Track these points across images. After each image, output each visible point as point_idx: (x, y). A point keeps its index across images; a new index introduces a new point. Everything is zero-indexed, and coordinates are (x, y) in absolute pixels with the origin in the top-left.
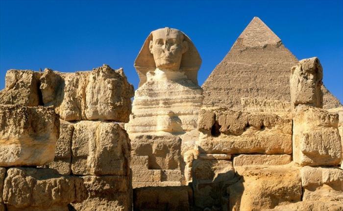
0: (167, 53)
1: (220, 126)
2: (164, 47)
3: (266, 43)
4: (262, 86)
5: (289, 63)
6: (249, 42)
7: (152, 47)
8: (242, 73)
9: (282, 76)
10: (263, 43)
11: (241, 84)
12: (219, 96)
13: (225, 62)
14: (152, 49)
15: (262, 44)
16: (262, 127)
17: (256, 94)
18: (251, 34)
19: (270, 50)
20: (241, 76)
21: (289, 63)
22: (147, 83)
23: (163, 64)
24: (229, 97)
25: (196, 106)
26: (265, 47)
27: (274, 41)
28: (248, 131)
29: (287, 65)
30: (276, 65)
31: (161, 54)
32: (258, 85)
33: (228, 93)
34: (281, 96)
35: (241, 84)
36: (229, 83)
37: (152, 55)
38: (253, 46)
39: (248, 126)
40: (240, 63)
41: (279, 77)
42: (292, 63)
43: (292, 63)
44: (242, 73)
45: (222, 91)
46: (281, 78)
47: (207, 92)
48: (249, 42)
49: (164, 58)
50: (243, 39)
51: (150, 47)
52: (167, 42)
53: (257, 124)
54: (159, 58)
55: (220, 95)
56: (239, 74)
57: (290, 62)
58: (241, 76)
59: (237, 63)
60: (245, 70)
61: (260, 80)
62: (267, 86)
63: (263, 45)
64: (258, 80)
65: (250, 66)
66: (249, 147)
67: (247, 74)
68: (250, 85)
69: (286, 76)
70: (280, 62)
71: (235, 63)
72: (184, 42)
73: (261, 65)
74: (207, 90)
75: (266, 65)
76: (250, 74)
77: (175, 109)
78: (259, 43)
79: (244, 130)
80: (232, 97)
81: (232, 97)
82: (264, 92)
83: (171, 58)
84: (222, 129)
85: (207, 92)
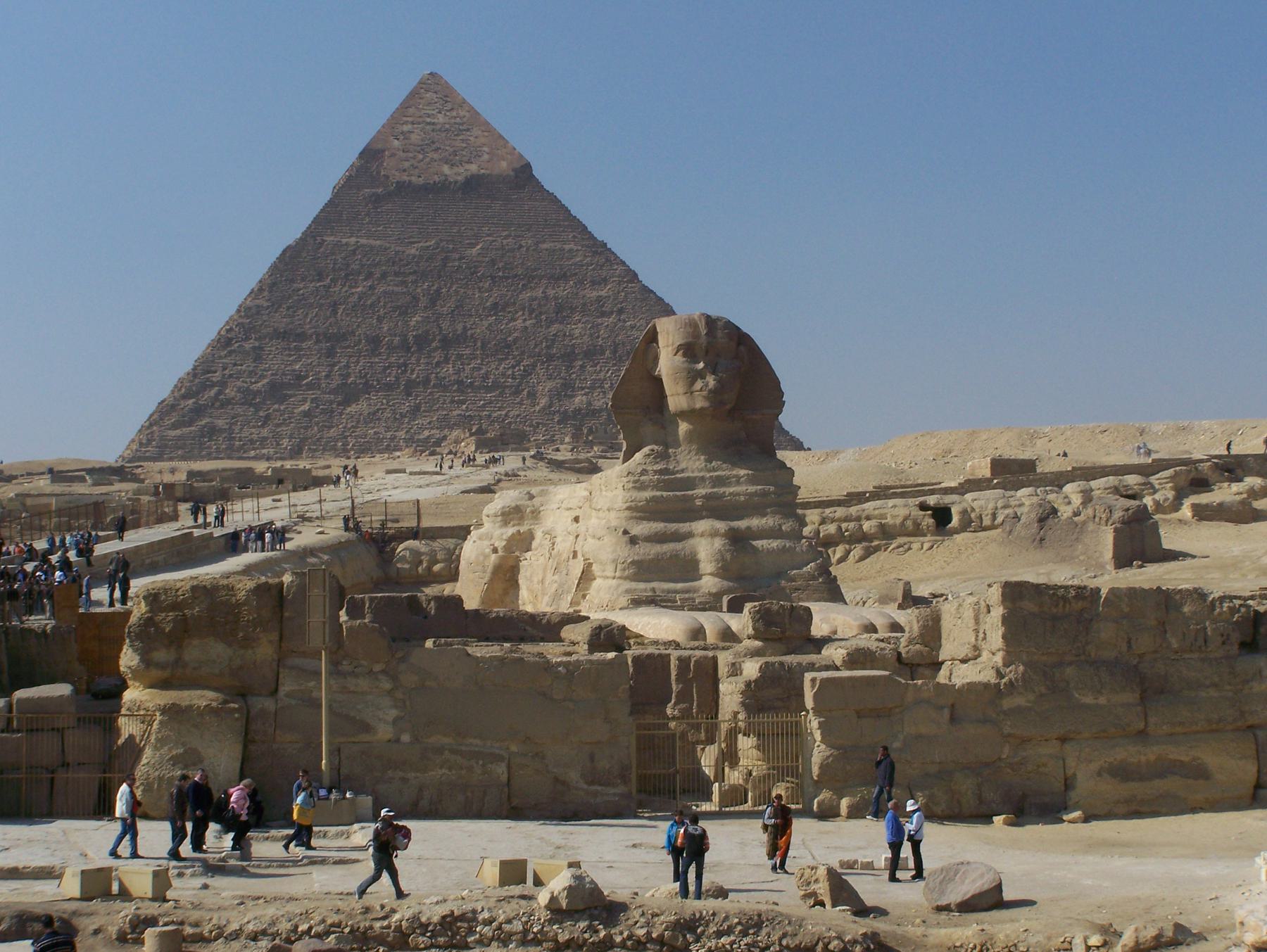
0: (711, 381)
2: (701, 365)
3: (473, 168)
4: (460, 327)
5: (559, 246)
6: (406, 164)
8: (384, 275)
11: (380, 320)
12: (296, 361)
13: (314, 238)
15: (456, 173)
17: (437, 356)
18: (414, 138)
20: (381, 289)
21: (559, 246)
23: (702, 409)
24: (334, 365)
27: (504, 164)
30: (512, 250)
31: (692, 383)
32: (445, 325)
33: (330, 353)
34: (534, 366)
35: (380, 320)
36: (335, 312)
37: (659, 381)
40: (372, 242)
41: (527, 295)
42: (572, 246)
43: (572, 246)
44: (384, 275)
46: (533, 299)
47: (248, 346)
48: (406, 164)
49: (705, 393)
50: (383, 151)
54: (689, 392)
55: (299, 359)
58: (381, 289)
59: (363, 241)
60: (396, 268)
61: (451, 304)
62: (481, 327)
64: (445, 308)
65: (413, 251)
67: (404, 283)
68: (412, 323)
69: (551, 292)
71: (353, 240)
72: (742, 348)
73: (454, 250)
74: (247, 339)
75: (474, 251)
76: (415, 282)
77: (742, 524)
78: (446, 169)
80: (347, 366)
81: (347, 366)
82: (468, 352)
83: (715, 395)
85: (248, 346)
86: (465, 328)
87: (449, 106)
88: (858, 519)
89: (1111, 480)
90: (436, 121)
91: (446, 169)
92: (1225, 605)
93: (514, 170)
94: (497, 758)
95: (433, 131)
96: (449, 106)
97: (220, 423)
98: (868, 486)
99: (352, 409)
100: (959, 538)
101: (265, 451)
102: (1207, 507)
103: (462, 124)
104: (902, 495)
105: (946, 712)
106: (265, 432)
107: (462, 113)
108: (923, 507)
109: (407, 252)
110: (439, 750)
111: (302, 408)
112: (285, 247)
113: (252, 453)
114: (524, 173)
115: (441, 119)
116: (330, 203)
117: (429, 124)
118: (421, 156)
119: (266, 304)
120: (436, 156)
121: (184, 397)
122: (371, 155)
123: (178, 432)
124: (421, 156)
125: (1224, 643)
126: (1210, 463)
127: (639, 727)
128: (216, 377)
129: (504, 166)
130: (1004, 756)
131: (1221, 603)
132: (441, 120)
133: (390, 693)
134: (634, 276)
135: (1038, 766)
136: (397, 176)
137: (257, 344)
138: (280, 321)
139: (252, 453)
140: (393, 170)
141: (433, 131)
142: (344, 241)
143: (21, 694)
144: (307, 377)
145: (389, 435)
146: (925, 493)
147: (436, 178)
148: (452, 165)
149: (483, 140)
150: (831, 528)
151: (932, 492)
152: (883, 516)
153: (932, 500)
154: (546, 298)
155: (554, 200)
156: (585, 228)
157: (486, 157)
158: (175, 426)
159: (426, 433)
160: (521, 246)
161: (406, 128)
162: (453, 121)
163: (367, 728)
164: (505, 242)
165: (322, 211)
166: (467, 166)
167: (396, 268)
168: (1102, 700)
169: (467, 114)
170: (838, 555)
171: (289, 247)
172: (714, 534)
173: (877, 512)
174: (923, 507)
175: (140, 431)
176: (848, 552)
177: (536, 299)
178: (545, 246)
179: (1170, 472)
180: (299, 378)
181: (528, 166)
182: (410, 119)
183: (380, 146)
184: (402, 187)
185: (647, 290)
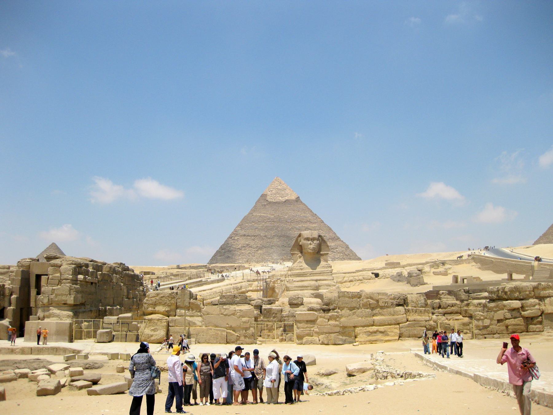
1: (441, 306)
3: (287, 198)
4: (283, 234)
6: (272, 197)
7: (300, 241)
9: (300, 226)
10: (284, 198)
14: (301, 243)
15: (283, 199)
16: (452, 306)
18: (273, 191)
19: (289, 204)
21: (306, 215)
22: (298, 262)
25: (329, 275)
26: (285, 202)
28: (449, 307)
29: (304, 216)
38: (275, 201)
39: (449, 306)
45: (248, 238)
47: (236, 238)
51: (299, 241)
52: (311, 239)
53: (451, 305)
56: (263, 224)
57: (307, 214)
59: (262, 215)
60: (269, 220)
63: (284, 200)
65: (273, 217)
66: (449, 312)
70: (299, 213)
71: (260, 214)
78: (280, 198)
79: (447, 307)
84: (442, 307)
85: (236, 238)
86: (284, 233)
87: (281, 184)
88: (358, 276)
89: (415, 266)
90: (278, 188)
91: (280, 198)
92: (392, 296)
93: (296, 198)
94: (224, 331)
95: (278, 190)
96: (281, 184)
97: (230, 255)
98: (361, 269)
99: (259, 252)
100: (381, 280)
101: (240, 262)
102: (437, 272)
103: (284, 188)
104: (368, 270)
105: (327, 320)
106: (240, 258)
107: (284, 186)
108: (372, 273)
109: (272, 217)
110: (211, 329)
111: (248, 252)
112: (244, 216)
113: (237, 262)
114: (298, 199)
115: (279, 187)
116: (255, 206)
117: (277, 188)
118: (275, 196)
119: (240, 229)
120: (278, 195)
121: (222, 250)
122: (264, 196)
123: (221, 257)
124: (275, 196)
125: (392, 305)
126: (438, 262)
127: (257, 324)
128: (230, 245)
129: (293, 198)
130: (341, 331)
131: (391, 295)
132: (279, 188)
133: (201, 316)
134: (323, 222)
135: (349, 333)
136: (270, 200)
137: (238, 238)
138: (243, 232)
139: (237, 262)
140: (268, 198)
141: (278, 190)
142: (258, 215)
143: (120, 316)
144: (249, 245)
145: (268, 258)
146: (373, 270)
147: (278, 200)
148: (282, 197)
149: (288, 192)
150: (351, 278)
151: (375, 270)
152: (364, 276)
153: (375, 272)
154: (302, 227)
155: (305, 205)
156: (311, 211)
157: (289, 195)
158: (220, 256)
159: (276, 257)
160: (297, 215)
161: (271, 189)
162: (282, 188)
163: (194, 324)
164: (293, 214)
165: (253, 208)
166: (285, 198)
167: (269, 220)
168: (363, 319)
169: (285, 186)
170: (353, 284)
171: (246, 216)
172: (313, 280)
173: (362, 275)
174: (372, 273)
175: (212, 257)
176: (356, 284)
177: (300, 227)
178: (302, 215)
179: (429, 264)
180: (248, 245)
181: (299, 197)
182: (273, 187)
183: (266, 194)
184: (270, 203)
185: (325, 224)
